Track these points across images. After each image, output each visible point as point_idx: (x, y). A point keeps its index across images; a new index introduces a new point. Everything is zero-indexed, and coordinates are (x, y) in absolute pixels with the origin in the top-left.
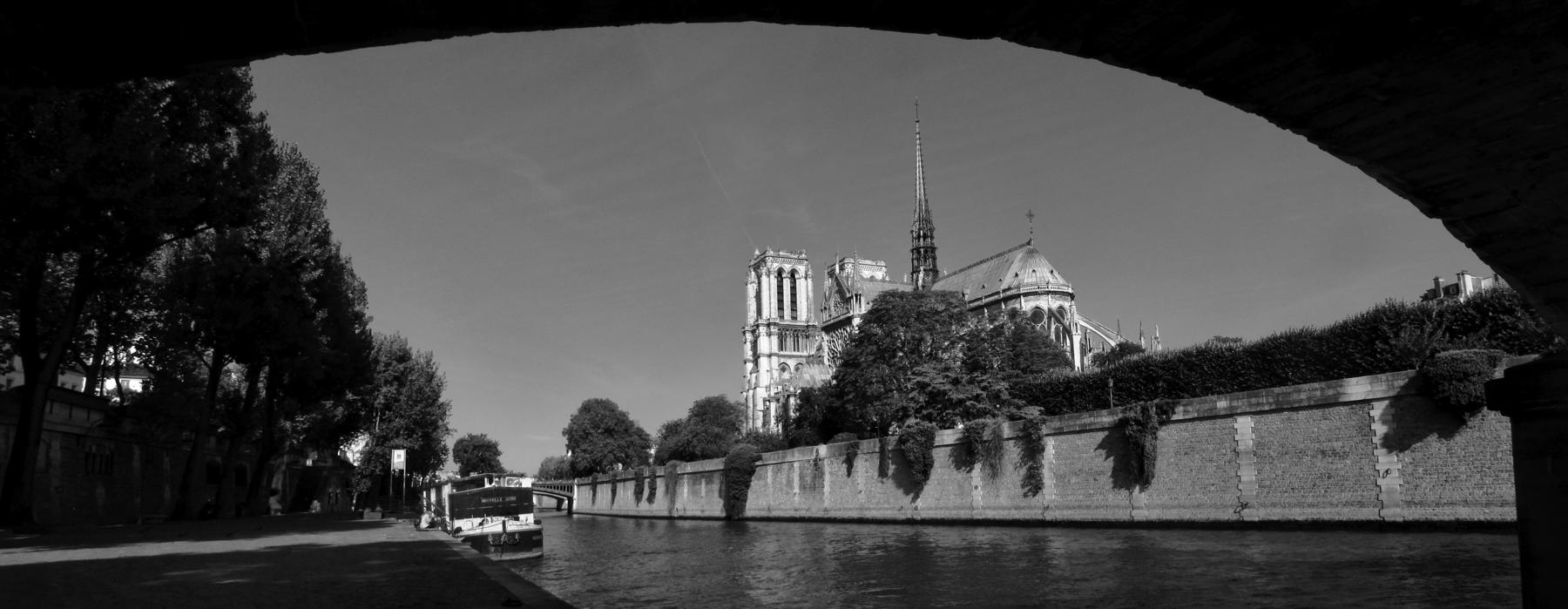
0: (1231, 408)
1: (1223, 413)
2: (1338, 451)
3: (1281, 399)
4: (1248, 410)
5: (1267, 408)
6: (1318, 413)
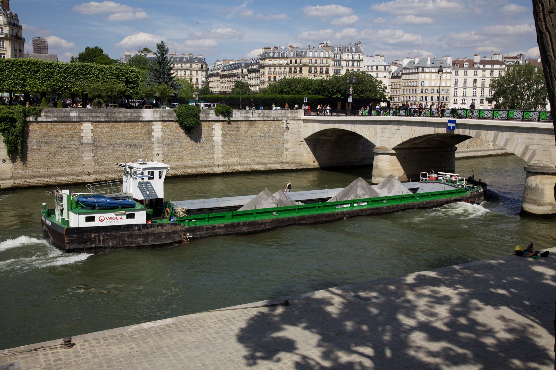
0: (79, 117)
1: (75, 120)
2: (137, 144)
3: (109, 115)
4: (91, 119)
5: (102, 120)
6: (128, 125)
